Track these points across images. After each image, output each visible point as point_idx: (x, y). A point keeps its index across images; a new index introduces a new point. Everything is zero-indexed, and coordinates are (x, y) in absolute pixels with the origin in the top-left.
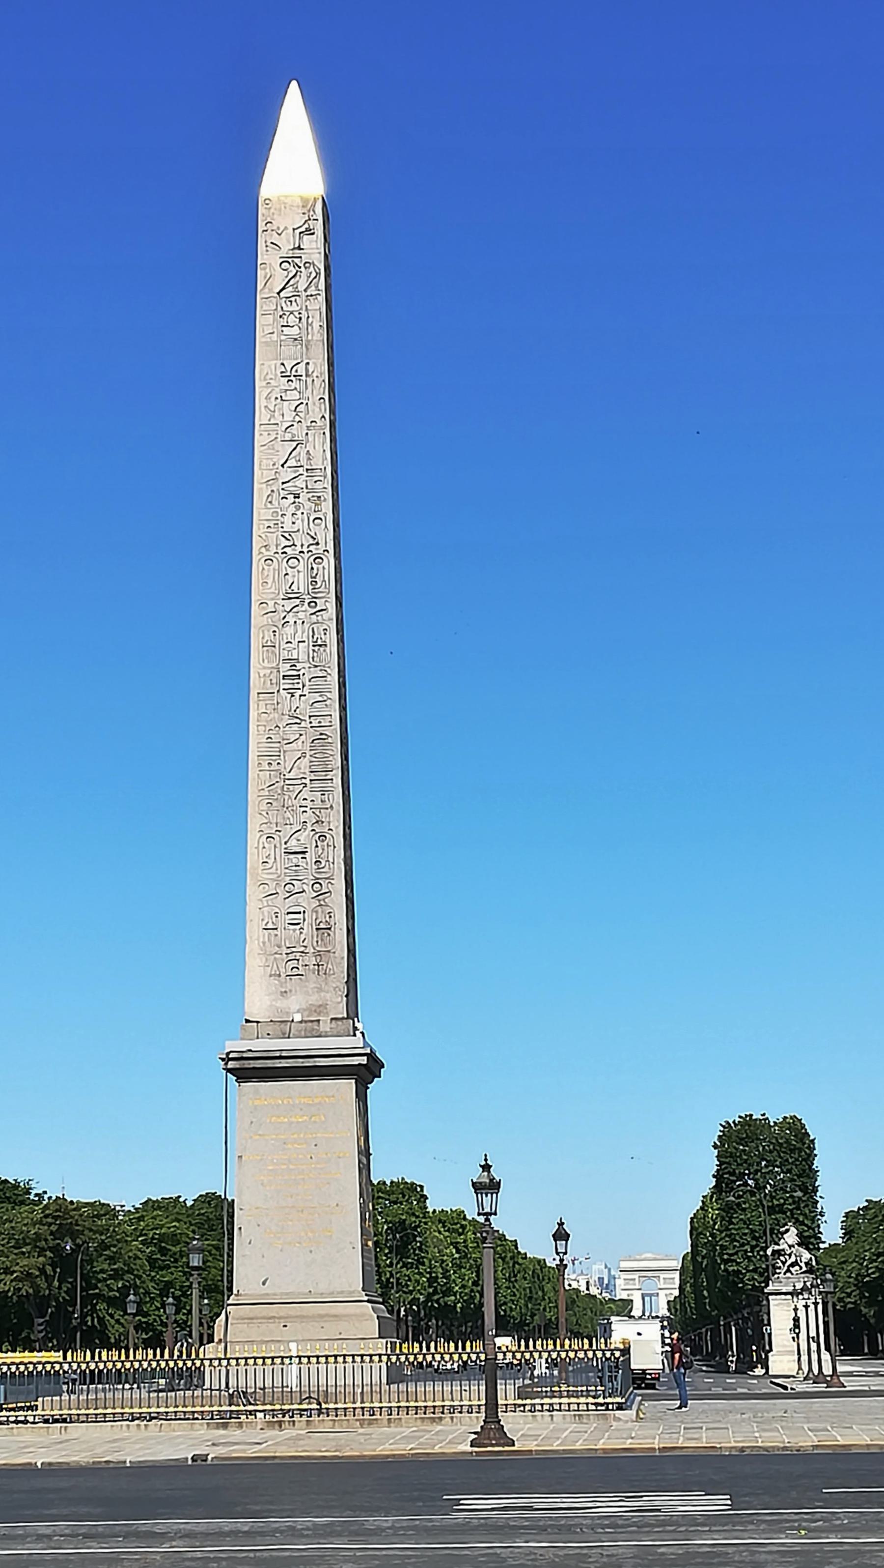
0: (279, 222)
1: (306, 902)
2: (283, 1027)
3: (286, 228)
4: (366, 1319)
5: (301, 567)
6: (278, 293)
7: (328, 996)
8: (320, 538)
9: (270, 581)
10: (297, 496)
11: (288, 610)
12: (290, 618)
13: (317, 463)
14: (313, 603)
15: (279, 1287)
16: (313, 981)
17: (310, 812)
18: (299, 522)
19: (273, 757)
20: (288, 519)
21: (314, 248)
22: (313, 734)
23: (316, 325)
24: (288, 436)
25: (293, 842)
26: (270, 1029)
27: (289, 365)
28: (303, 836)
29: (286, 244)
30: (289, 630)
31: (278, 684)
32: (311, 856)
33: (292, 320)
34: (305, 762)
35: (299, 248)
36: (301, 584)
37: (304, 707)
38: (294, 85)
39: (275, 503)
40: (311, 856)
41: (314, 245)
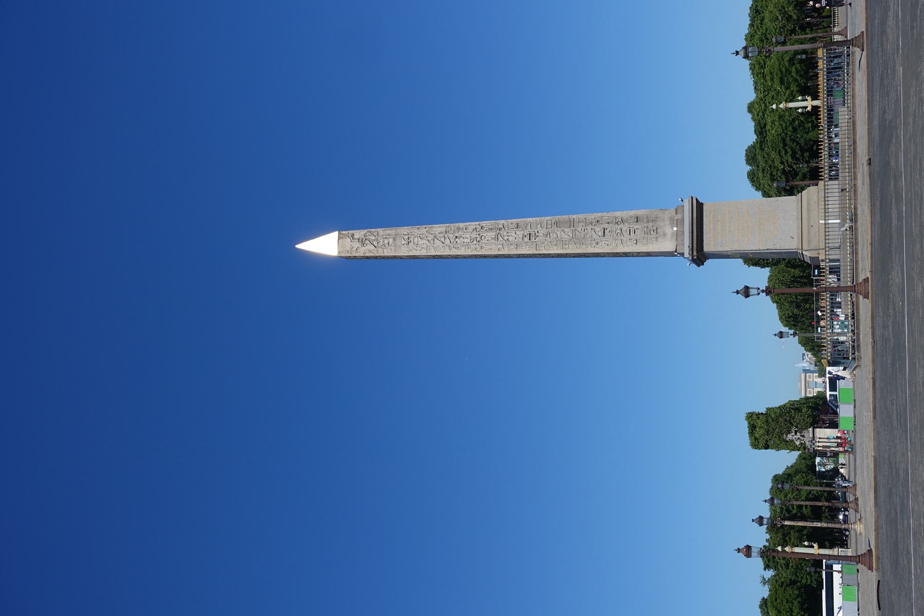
1: (625, 227)
2: (679, 235)
4: (811, 193)
12: (506, 238)
13: (443, 229)
14: (500, 229)
15: (795, 232)
16: (660, 224)
19: (564, 243)
20: (466, 240)
21: (359, 234)
22: (554, 227)
26: (680, 240)
28: (597, 229)
29: (357, 245)
30: (511, 238)
32: (606, 226)
33: (386, 241)
36: (492, 234)
37: (542, 232)
38: (297, 246)
40: (606, 226)
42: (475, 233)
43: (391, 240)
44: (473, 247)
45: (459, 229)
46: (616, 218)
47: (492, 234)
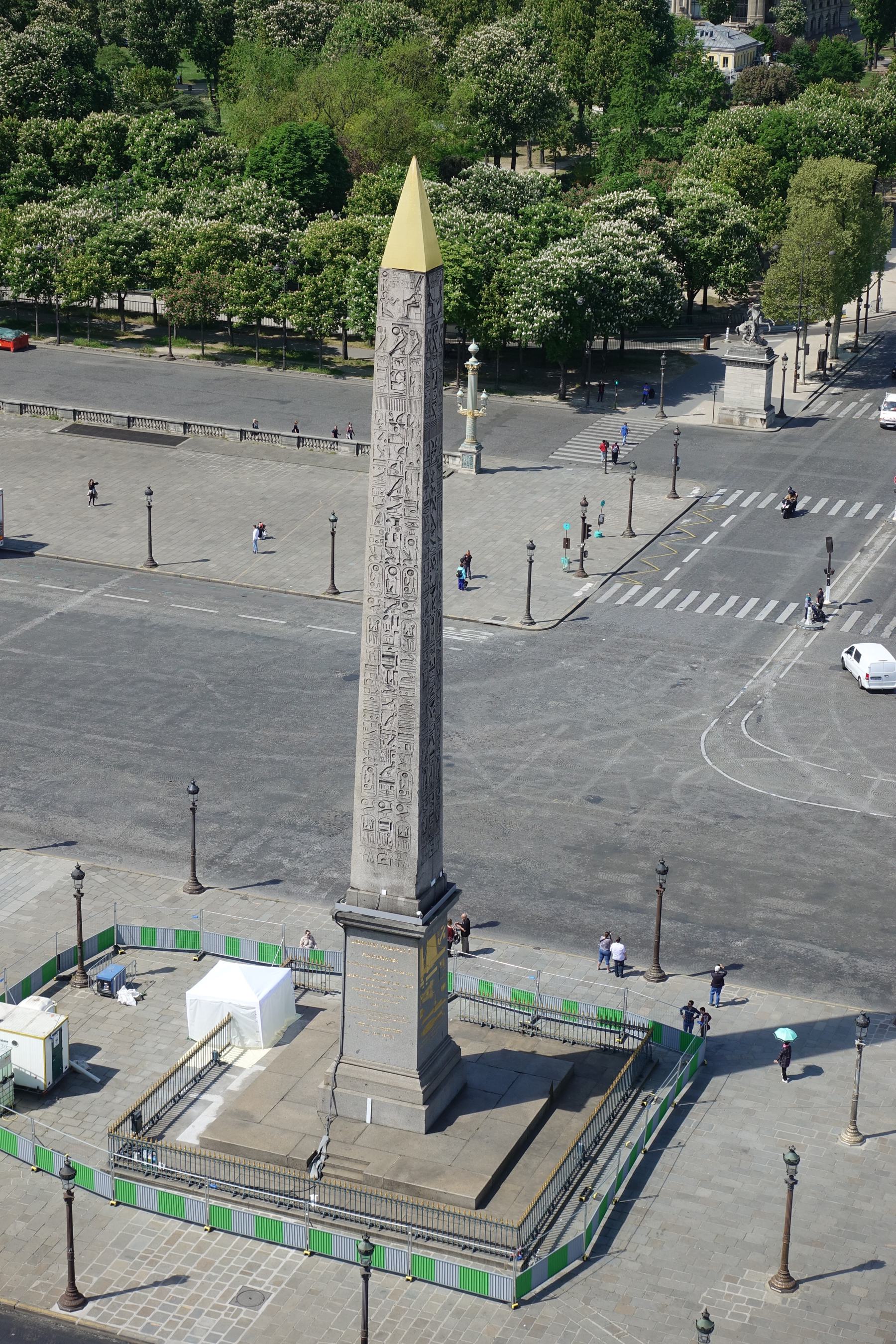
0: (394, 293)
1: (392, 817)
3: (398, 300)
5: (398, 576)
7: (405, 882)
8: (413, 556)
9: (376, 582)
10: (397, 521)
11: (388, 605)
12: (390, 614)
14: (405, 605)
17: (396, 757)
18: (398, 541)
20: (390, 537)
22: (400, 701)
23: (417, 384)
24: (393, 472)
25: (385, 774)
27: (396, 414)
28: (393, 771)
29: (397, 312)
30: (388, 621)
31: (379, 660)
32: (396, 787)
33: (400, 377)
34: (396, 720)
36: (398, 590)
39: (382, 523)
40: (396, 787)
41: (418, 317)
43: (400, 388)
44: (378, 551)
45: (412, 526)
46: (409, 803)
47: (398, 590)
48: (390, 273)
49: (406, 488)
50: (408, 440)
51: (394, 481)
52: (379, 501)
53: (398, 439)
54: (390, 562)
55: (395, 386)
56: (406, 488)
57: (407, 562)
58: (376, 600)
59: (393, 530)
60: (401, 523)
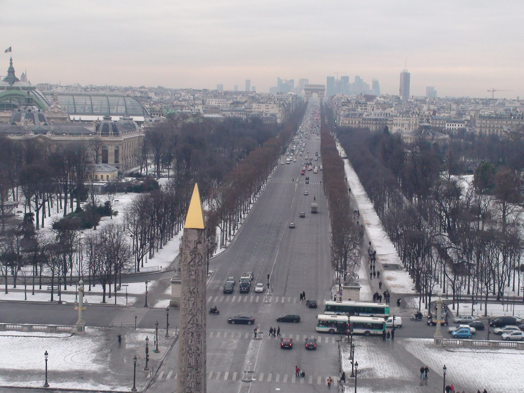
5: (193, 357)
6: (189, 263)
8: (200, 348)
9: (183, 361)
10: (193, 333)
11: (189, 370)
12: (190, 374)
14: (197, 369)
18: (193, 342)
20: (190, 341)
24: (190, 313)
27: (191, 289)
30: (189, 378)
33: (193, 273)
35: (196, 248)
36: (193, 363)
42: (195, 349)
43: (194, 277)
48: (189, 230)
49: (197, 319)
50: (197, 299)
51: (191, 317)
52: (185, 326)
53: (193, 299)
54: (190, 351)
55: (191, 277)
56: (197, 319)
57: (197, 351)
58: (183, 369)
59: (191, 338)
60: (194, 334)
